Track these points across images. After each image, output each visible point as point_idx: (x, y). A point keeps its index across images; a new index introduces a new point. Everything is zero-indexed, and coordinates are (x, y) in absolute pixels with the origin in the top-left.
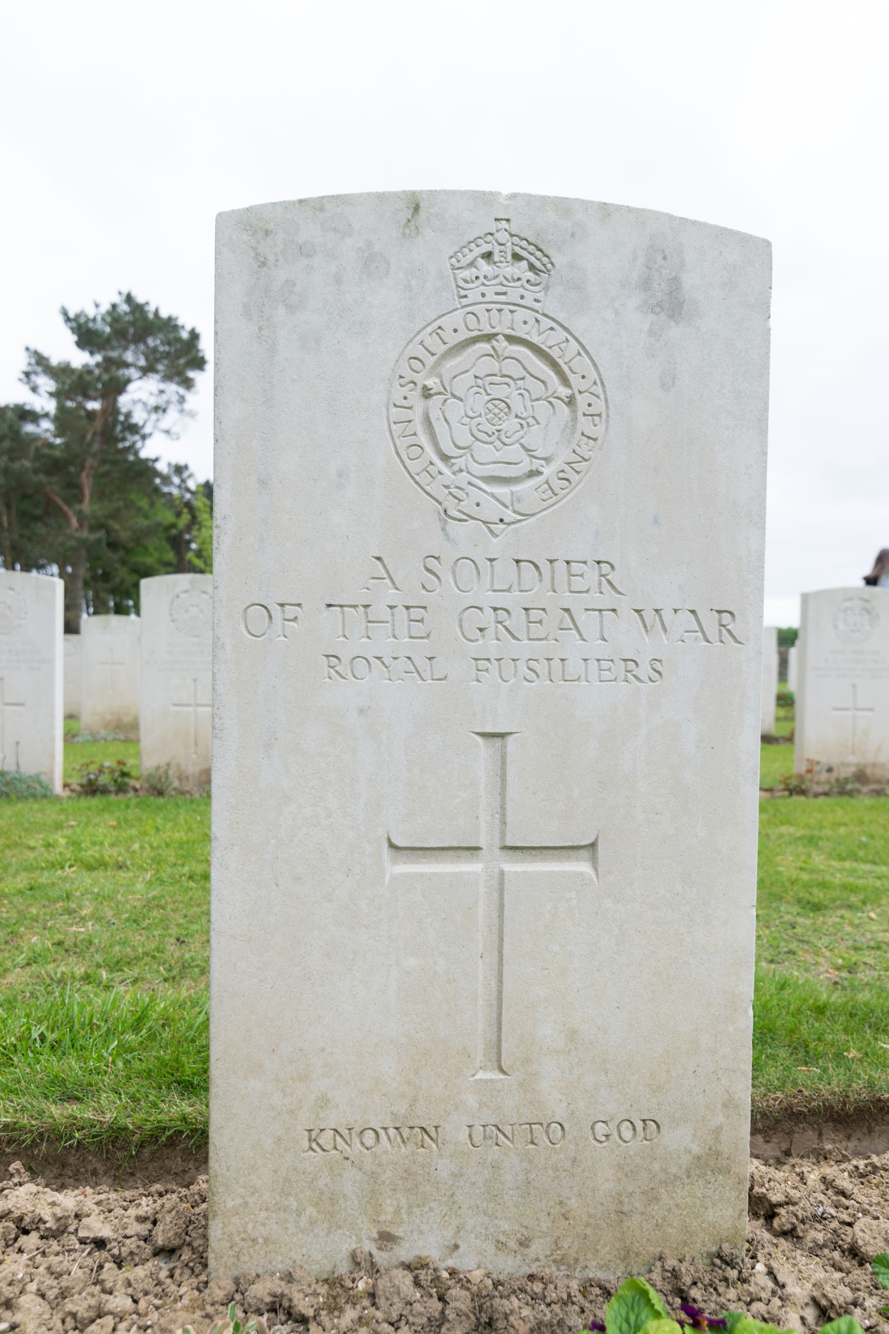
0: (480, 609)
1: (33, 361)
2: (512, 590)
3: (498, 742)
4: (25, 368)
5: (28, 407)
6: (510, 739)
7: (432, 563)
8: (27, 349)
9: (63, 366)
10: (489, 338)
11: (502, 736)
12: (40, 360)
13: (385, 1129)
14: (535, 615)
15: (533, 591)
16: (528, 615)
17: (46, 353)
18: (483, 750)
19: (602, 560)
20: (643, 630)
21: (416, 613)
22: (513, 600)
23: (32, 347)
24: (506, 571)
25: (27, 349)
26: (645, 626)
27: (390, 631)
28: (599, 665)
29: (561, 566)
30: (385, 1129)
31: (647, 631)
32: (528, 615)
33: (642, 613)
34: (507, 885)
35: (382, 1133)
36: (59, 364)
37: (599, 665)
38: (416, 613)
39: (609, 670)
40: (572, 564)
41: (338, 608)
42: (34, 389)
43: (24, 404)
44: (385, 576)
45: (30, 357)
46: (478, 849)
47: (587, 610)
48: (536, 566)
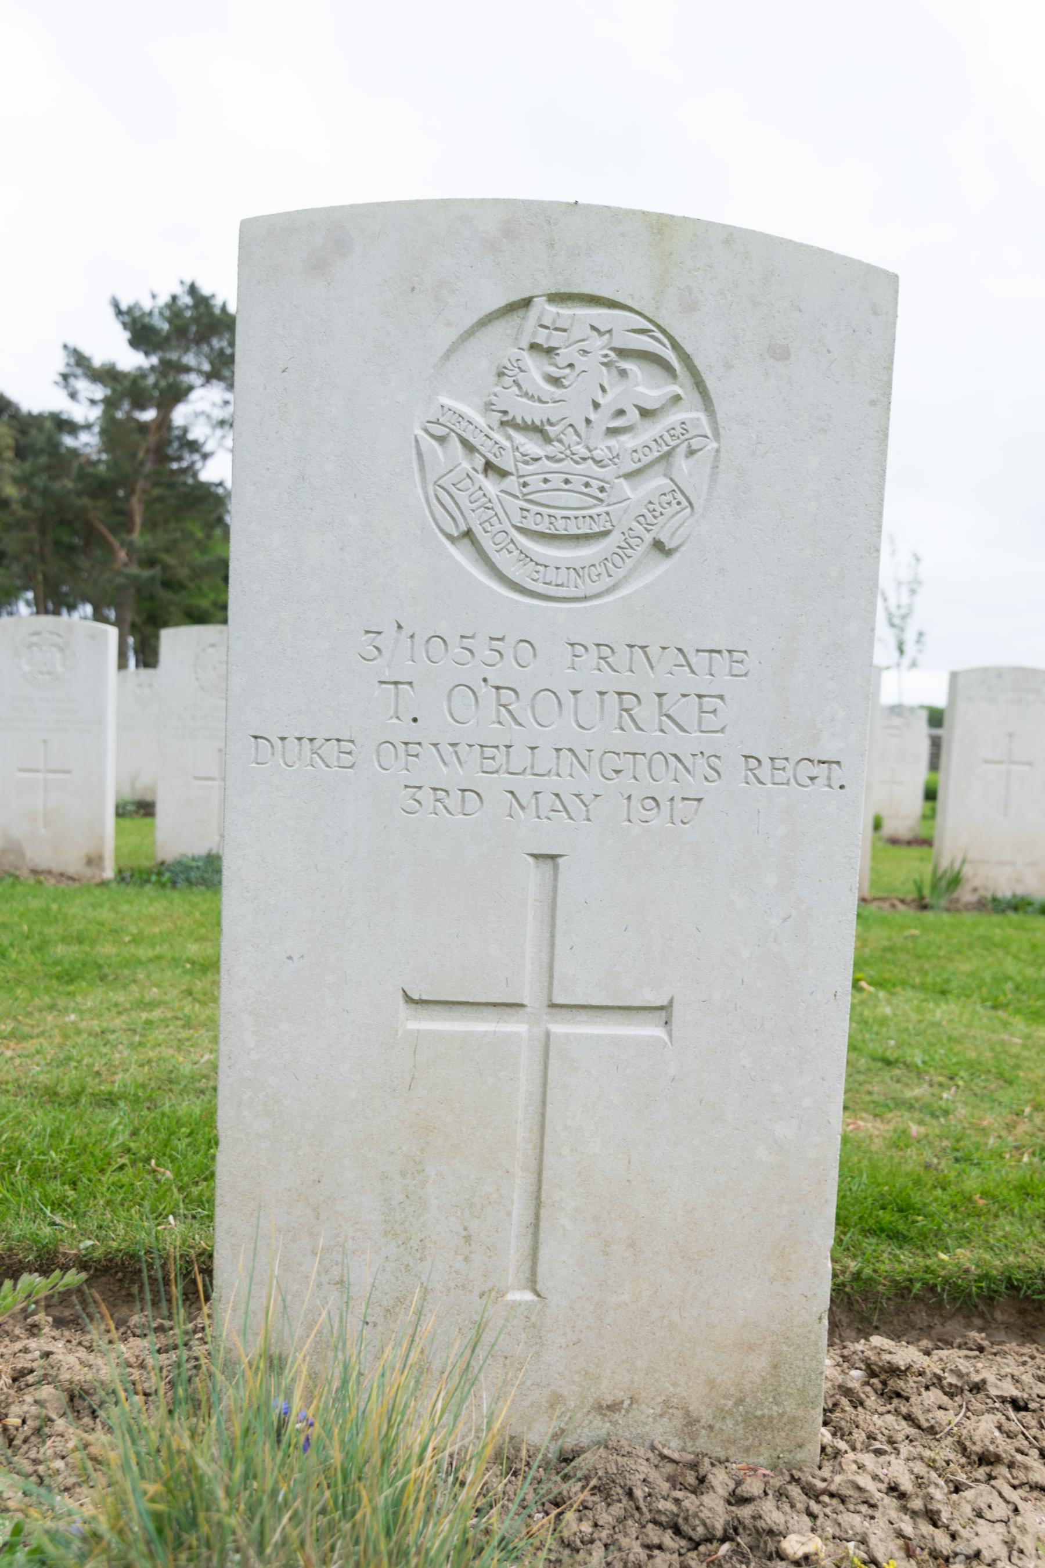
1: (72, 361)
4: (63, 369)
5: (64, 417)
8: (65, 347)
10: (527, 303)
12: (80, 360)
17: (87, 350)
23: (71, 344)
25: (65, 347)
28: (482, 752)
36: (103, 365)
37: (482, 752)
39: (493, 758)
42: (73, 395)
43: (61, 412)
45: (68, 356)
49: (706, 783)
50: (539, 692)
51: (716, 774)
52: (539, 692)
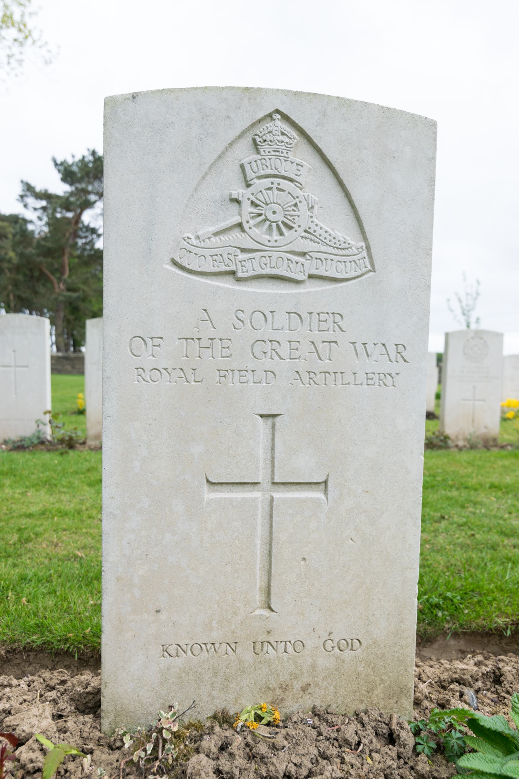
1: (25, 188)
3: (270, 421)
4: (21, 193)
5: (21, 216)
7: (240, 314)
8: (22, 182)
9: (43, 192)
12: (29, 188)
13: (205, 644)
15: (297, 331)
17: (33, 184)
20: (366, 357)
21: (226, 343)
22: (283, 336)
23: (26, 180)
25: (22, 182)
29: (315, 316)
30: (205, 644)
34: (275, 503)
35: (203, 646)
36: (40, 191)
38: (226, 343)
40: (321, 314)
42: (26, 206)
43: (19, 214)
44: (208, 319)
45: (23, 186)
50: (138, 337)
52: (138, 337)
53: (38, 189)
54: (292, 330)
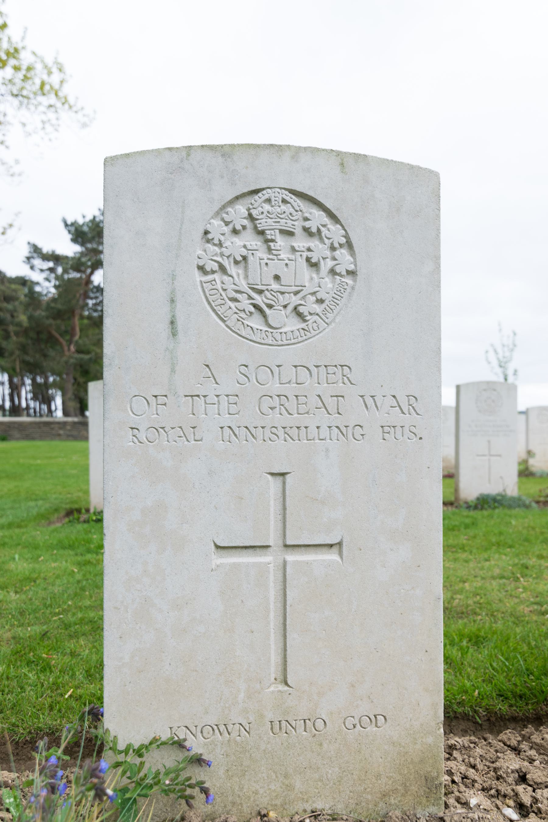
0: (271, 397)
1: (32, 250)
2: (291, 383)
4: (27, 255)
5: (27, 278)
6: (288, 476)
8: (29, 243)
9: (50, 253)
11: (283, 475)
12: (36, 250)
14: (302, 399)
16: (298, 399)
17: (40, 245)
18: (274, 484)
19: (298, 365)
23: (32, 241)
24: (289, 373)
25: (29, 243)
26: (376, 406)
27: (217, 411)
31: (378, 409)
32: (298, 399)
33: (364, 397)
36: (47, 252)
41: (190, 398)
42: (32, 268)
43: (25, 276)
46: (268, 547)
47: (331, 396)
48: (308, 369)
49: (270, 442)
51: (276, 437)
53: (45, 251)
54: (283, 384)
